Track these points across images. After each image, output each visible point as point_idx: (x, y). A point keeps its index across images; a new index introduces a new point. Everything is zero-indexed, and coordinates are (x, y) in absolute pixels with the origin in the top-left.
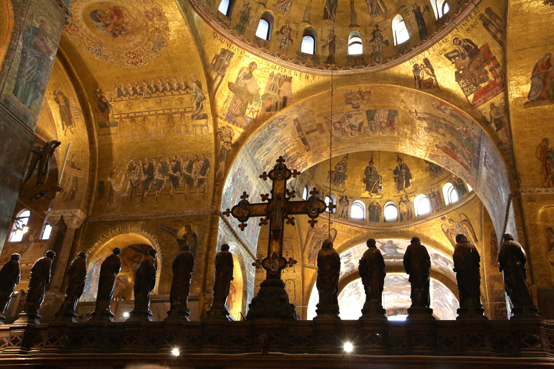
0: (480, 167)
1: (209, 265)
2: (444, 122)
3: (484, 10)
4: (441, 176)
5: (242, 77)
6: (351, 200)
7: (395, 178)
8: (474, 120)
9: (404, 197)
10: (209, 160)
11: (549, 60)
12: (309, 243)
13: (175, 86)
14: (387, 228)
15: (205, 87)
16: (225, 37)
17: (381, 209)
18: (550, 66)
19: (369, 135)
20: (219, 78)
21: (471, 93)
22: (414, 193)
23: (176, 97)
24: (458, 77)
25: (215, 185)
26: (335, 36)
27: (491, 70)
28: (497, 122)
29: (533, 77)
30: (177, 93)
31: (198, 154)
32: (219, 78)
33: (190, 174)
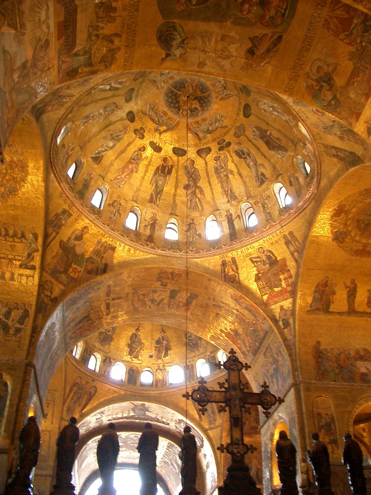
0: (258, 355)
1: (19, 417)
2: (236, 312)
3: (288, 232)
4: (197, 352)
5: (73, 237)
6: (114, 361)
7: (156, 347)
8: (266, 316)
9: (161, 365)
10: (29, 311)
11: (327, 281)
12: (70, 397)
13: (11, 232)
14: (143, 392)
15: (40, 239)
16: (69, 198)
17: (139, 373)
18: (327, 286)
19: (164, 311)
20: (54, 234)
21: (266, 294)
22: (171, 363)
23: (9, 243)
24: (258, 279)
25: (32, 336)
26: (157, 220)
27: (285, 279)
28: (284, 322)
29: (315, 292)
30: (12, 239)
31: (19, 303)
32: (54, 234)
33: (7, 321)
